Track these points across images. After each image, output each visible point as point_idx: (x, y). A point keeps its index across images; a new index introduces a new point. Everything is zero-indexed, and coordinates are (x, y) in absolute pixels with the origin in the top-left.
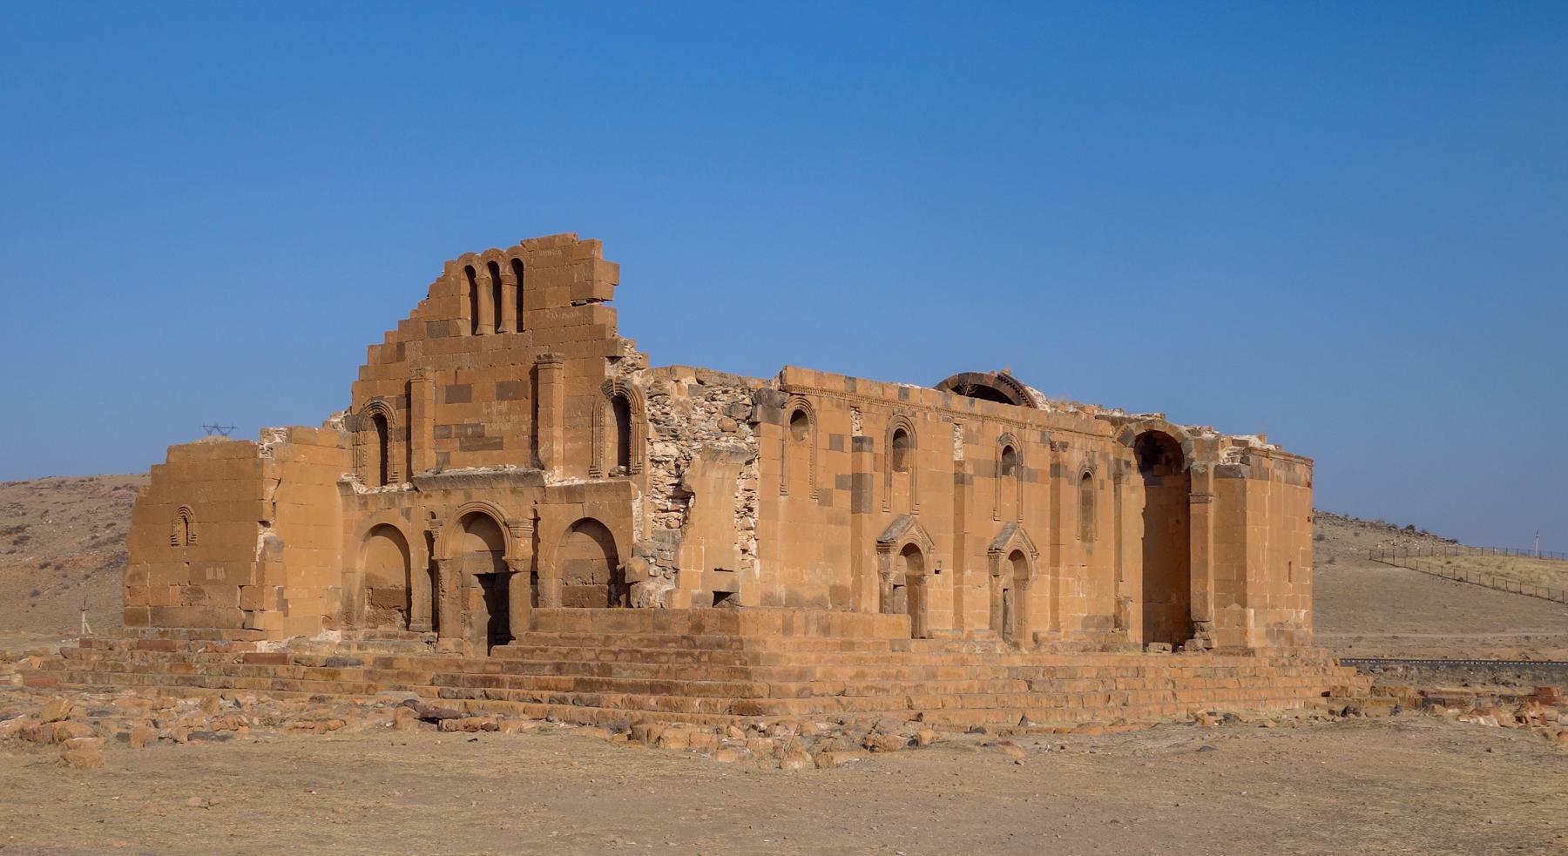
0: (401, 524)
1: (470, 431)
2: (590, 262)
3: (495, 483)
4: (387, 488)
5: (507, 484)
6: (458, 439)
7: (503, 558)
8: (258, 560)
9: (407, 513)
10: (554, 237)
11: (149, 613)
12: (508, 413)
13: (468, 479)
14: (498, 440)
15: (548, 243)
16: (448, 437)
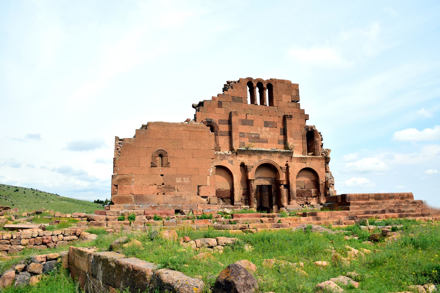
0: (229, 166)
1: (253, 136)
2: (297, 91)
3: (273, 154)
4: (219, 153)
5: (278, 155)
6: (248, 138)
7: (280, 179)
8: (210, 175)
9: (231, 162)
10: (285, 80)
11: (133, 198)
12: (270, 131)
13: (261, 152)
14: (265, 140)
15: (282, 82)
16: (244, 136)
